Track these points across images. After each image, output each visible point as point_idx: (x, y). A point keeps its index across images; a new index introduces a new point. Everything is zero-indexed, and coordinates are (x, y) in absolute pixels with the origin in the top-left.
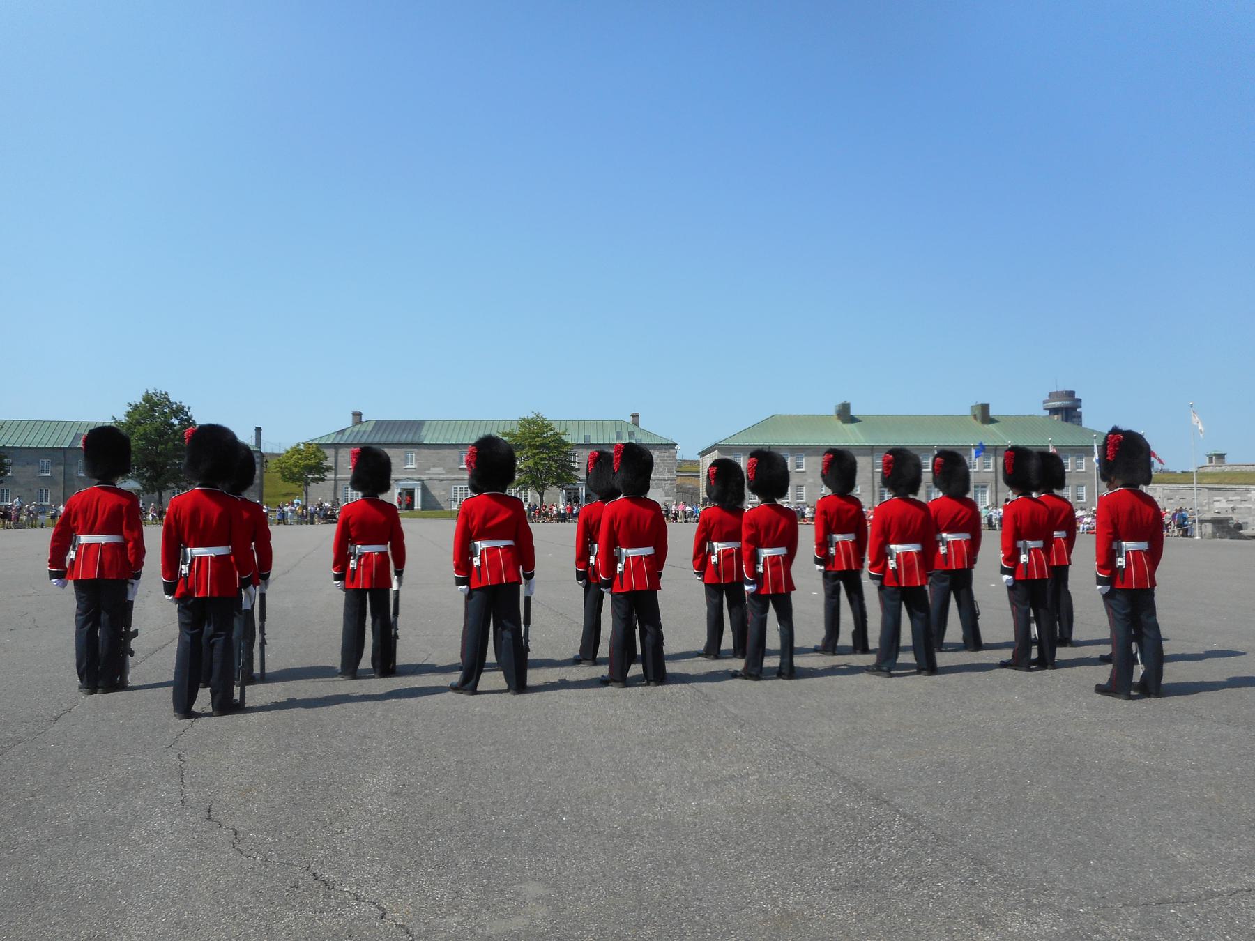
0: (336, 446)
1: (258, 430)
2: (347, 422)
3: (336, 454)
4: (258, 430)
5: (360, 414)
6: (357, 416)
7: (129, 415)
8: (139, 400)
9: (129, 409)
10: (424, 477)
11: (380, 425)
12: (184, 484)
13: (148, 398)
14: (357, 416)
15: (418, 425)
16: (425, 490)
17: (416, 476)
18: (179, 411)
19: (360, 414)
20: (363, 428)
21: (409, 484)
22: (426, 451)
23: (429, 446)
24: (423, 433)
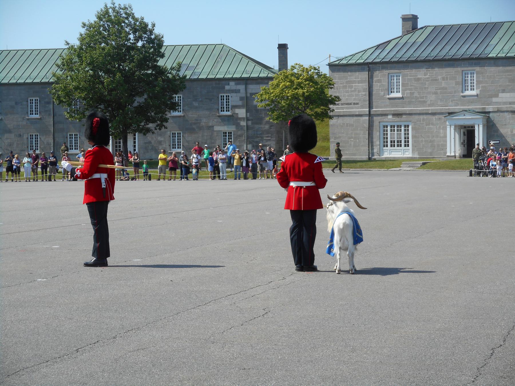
0: (369, 67)
1: (283, 48)
2: (395, 29)
3: (371, 78)
4: (283, 48)
5: (414, 19)
6: (411, 22)
7: (82, 39)
8: (93, 19)
9: (83, 31)
10: (489, 108)
11: (440, 32)
12: (151, 126)
13: (104, 15)
14: (411, 22)
15: (492, 28)
16: (491, 129)
17: (478, 107)
18: (142, 28)
19: (414, 19)
20: (419, 37)
21: (467, 119)
22: (491, 70)
23: (497, 61)
24: (494, 42)
